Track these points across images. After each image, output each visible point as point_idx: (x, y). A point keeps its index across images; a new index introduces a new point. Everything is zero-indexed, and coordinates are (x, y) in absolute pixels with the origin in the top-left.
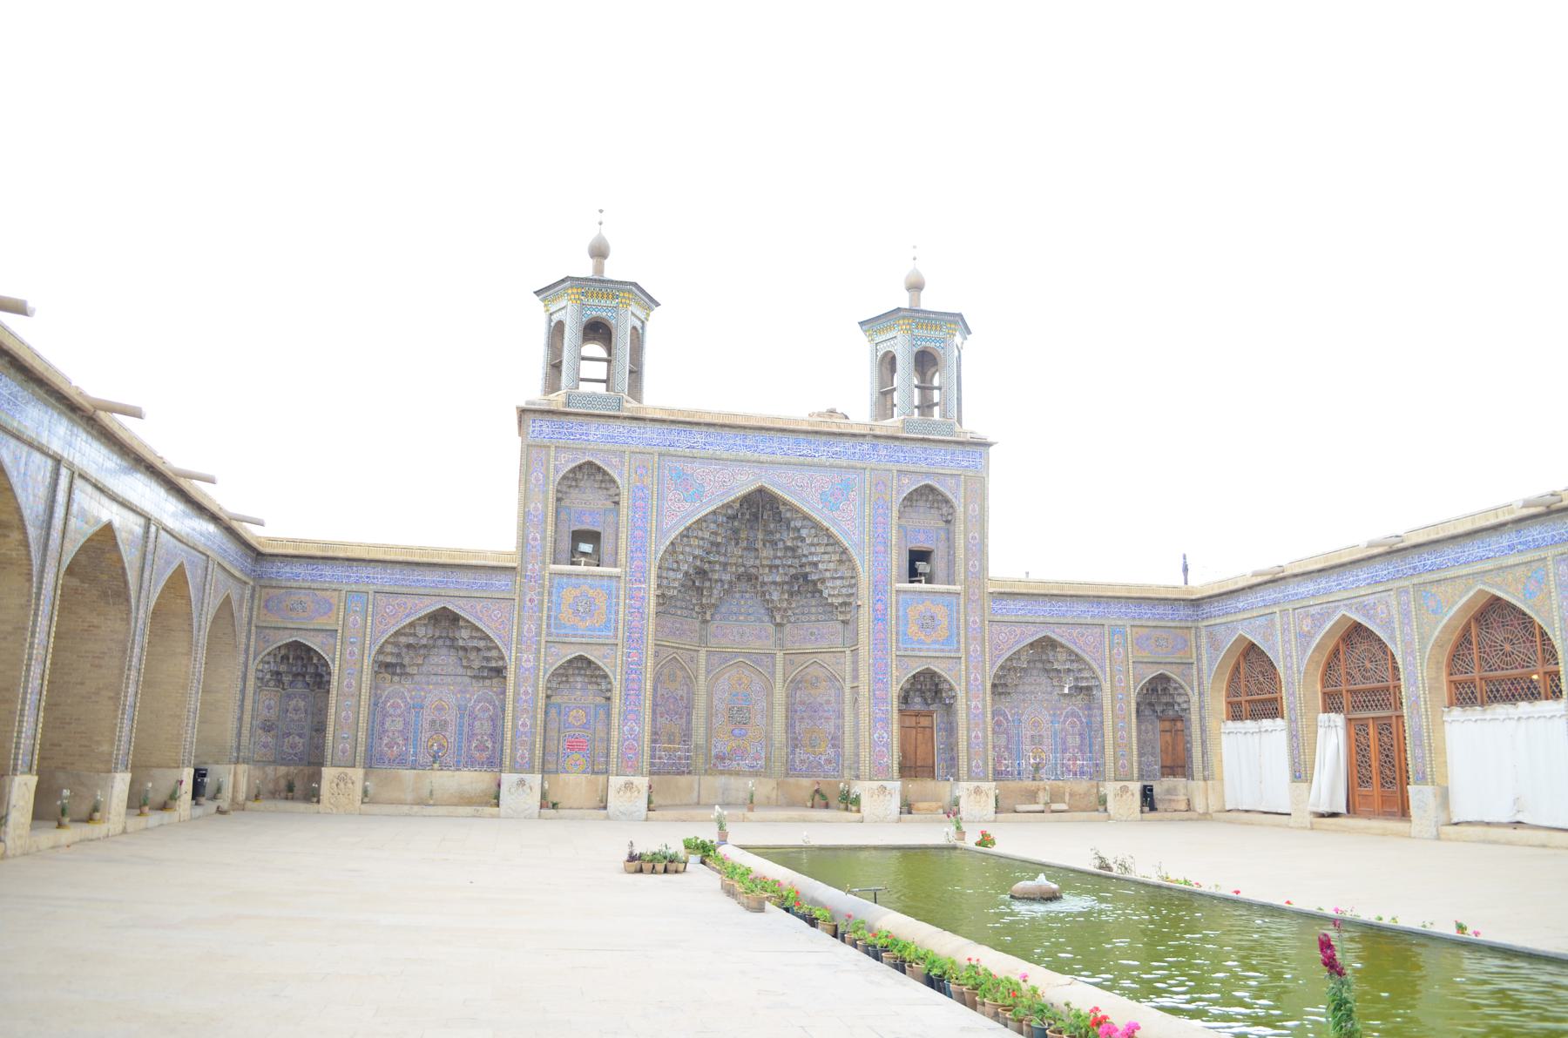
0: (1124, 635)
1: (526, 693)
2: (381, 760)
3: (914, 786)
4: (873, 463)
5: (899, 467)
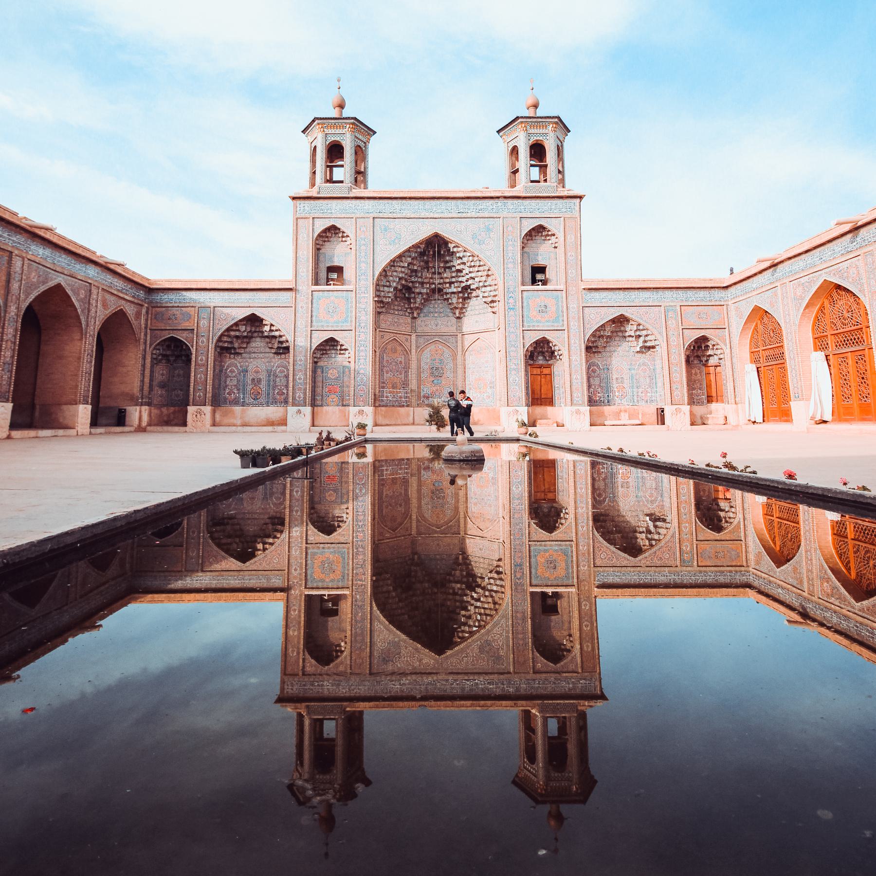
0: (675, 311)
1: (301, 360)
2: (225, 402)
3: (539, 410)
4: (505, 214)
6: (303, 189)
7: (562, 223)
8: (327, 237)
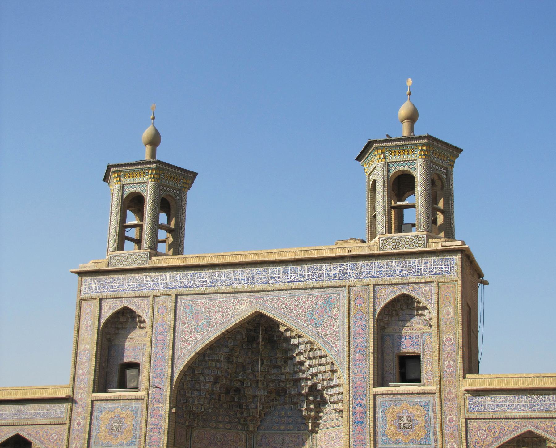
4: (352, 281)
5: (374, 281)
6: (104, 254)
7: (435, 291)
8: (121, 323)
